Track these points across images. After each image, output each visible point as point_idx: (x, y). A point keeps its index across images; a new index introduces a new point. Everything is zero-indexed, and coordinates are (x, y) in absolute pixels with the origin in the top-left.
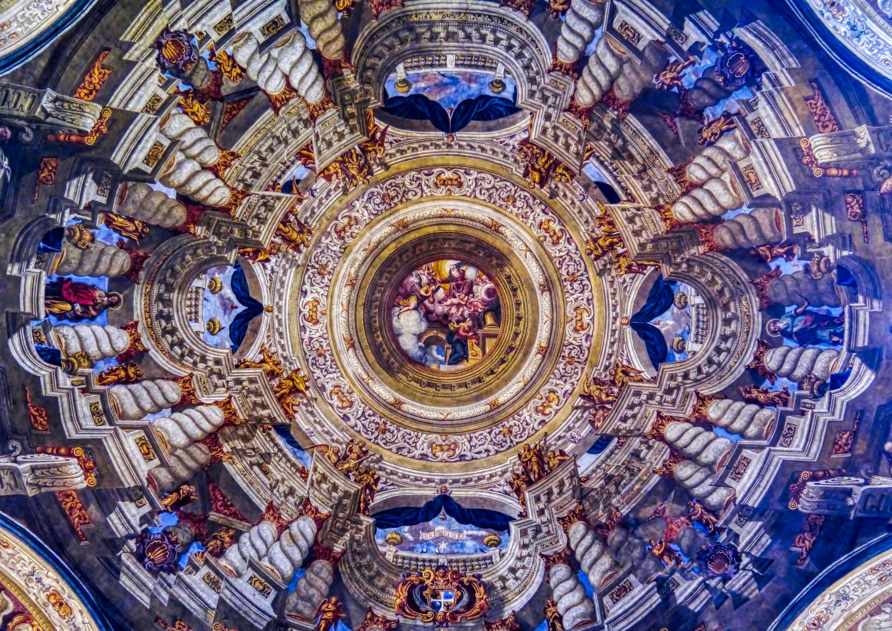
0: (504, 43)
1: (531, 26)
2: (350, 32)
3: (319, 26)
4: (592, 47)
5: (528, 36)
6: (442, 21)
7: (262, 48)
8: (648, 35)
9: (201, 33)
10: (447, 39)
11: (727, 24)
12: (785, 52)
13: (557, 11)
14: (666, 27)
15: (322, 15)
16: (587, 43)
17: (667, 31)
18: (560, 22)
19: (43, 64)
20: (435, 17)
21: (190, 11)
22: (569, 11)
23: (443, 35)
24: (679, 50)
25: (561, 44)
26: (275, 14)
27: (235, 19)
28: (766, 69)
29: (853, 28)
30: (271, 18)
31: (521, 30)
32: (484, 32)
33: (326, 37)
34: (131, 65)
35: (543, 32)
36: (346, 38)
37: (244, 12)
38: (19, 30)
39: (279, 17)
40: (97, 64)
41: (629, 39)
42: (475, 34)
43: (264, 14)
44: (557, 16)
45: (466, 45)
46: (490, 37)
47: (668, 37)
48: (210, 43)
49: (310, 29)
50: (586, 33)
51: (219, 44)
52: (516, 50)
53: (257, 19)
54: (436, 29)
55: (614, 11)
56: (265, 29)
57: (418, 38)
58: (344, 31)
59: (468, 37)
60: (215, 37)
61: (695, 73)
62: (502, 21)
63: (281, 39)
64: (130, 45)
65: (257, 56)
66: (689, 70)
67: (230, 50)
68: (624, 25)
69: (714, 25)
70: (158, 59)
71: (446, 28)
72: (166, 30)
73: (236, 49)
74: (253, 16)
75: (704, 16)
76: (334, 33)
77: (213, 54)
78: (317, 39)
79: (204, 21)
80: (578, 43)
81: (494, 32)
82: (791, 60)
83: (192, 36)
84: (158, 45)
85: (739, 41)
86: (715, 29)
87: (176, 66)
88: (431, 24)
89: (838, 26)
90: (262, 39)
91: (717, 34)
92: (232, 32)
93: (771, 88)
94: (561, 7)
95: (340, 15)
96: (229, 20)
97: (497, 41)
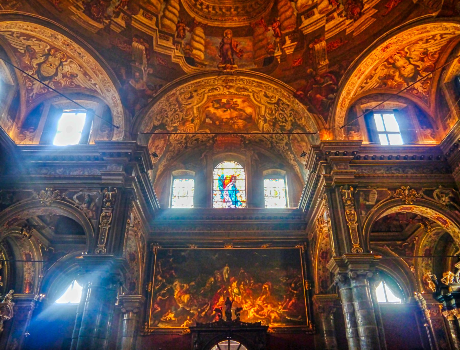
0: (204, 7)
1: (192, 15)
2: (275, 12)
3: (288, 13)
4: (163, 6)
5: (193, 10)
6: (233, 16)
7: (316, 6)
8: (140, 17)
9: (341, 17)
10: (231, 8)
11: (107, 29)
12: (78, 21)
13: (182, 23)
14: (133, 22)
15: (286, 19)
16: (166, 8)
17: (132, 20)
18: (180, 17)
19: (412, 15)
20: (236, 18)
21: (343, 27)
22: (177, 23)
23: (232, 10)
24: (124, 13)
25: (178, 6)
26: (307, 20)
27: (325, 21)
28: (84, 12)
29: (55, 38)
30: (309, 19)
31: (197, 13)
32: (214, 12)
33: (287, 7)
34: (375, 7)
35: (187, 12)
36: (277, 8)
37: (320, 23)
38: (415, 32)
39: (306, 19)
40: (389, 10)
41: (148, 14)
42: (218, 10)
43: (312, 21)
44: (182, 20)
45: (222, 5)
46: (211, 9)
47: (131, 18)
48: (338, 12)
49: (293, 12)
50: (167, 13)
51: (335, 11)
52: (198, 3)
53: (315, 20)
54: (236, 12)
55: (157, 25)
56: (313, 14)
57: (244, 8)
58: (278, 11)
59: (221, 9)
60: (335, 14)
61: (114, 3)
62: (206, 17)
63: (307, 8)
64: (372, 17)
65: (318, 2)
66: (117, 4)
67: (330, 7)
68: (151, 19)
69: (112, 27)
70: (363, 8)
71: (231, 13)
72: (355, 20)
73: (327, 7)
74: (317, 21)
75: (118, 30)
76: (282, 10)
77: (338, 6)
78: (290, 7)
79: (338, 22)
80: (170, 8)
81: (209, 12)
82: (75, 18)
83: (345, 16)
84: (361, 14)
85: (100, 22)
86: (112, 25)
87: (356, 3)
88: (238, 15)
89: (62, 38)
90: (315, 10)
91: (110, 23)
92: (327, 15)
93: (78, 4)
94: (181, 24)
95: (278, 19)
96: (327, 21)
97: (208, 7)
